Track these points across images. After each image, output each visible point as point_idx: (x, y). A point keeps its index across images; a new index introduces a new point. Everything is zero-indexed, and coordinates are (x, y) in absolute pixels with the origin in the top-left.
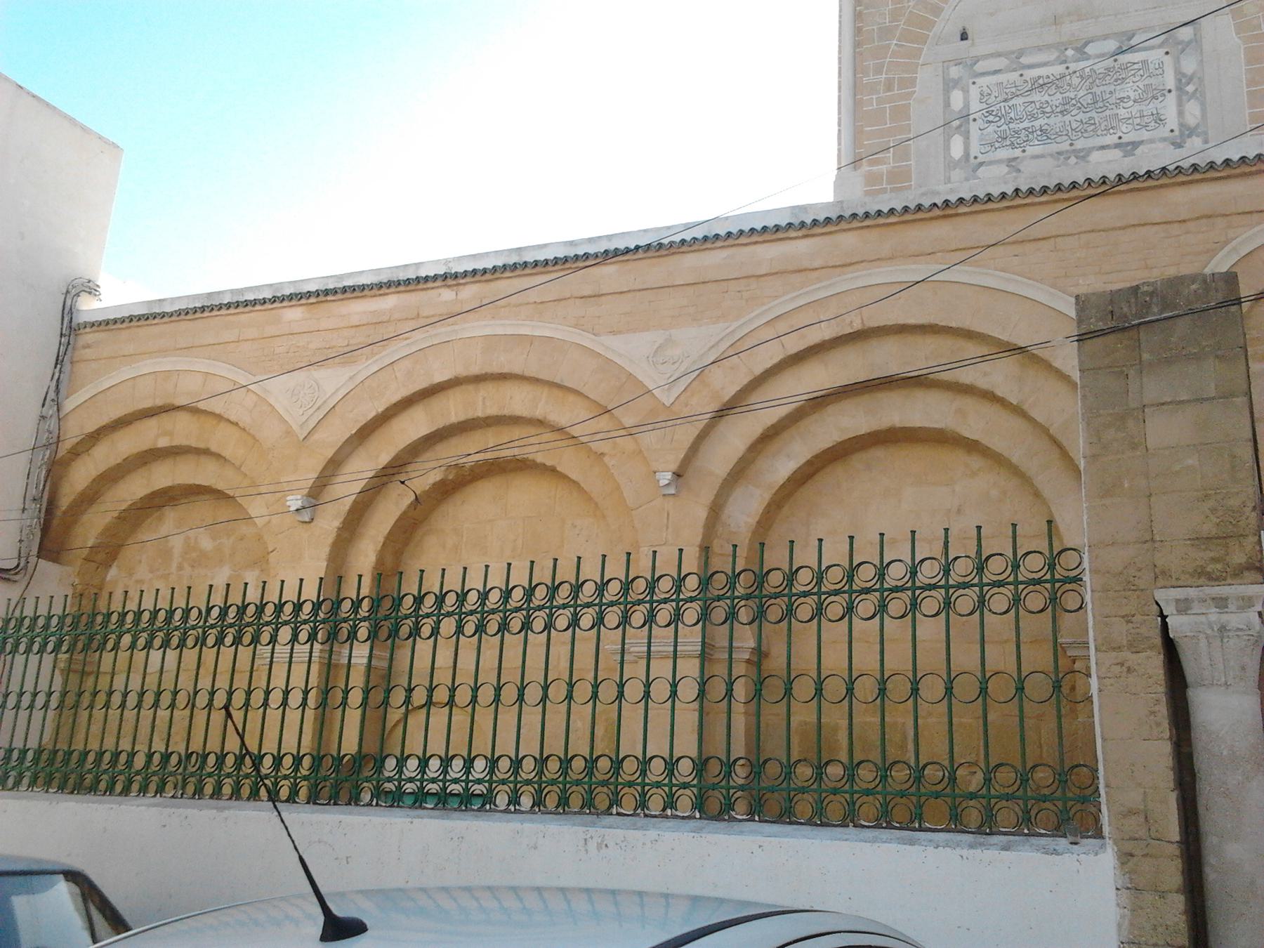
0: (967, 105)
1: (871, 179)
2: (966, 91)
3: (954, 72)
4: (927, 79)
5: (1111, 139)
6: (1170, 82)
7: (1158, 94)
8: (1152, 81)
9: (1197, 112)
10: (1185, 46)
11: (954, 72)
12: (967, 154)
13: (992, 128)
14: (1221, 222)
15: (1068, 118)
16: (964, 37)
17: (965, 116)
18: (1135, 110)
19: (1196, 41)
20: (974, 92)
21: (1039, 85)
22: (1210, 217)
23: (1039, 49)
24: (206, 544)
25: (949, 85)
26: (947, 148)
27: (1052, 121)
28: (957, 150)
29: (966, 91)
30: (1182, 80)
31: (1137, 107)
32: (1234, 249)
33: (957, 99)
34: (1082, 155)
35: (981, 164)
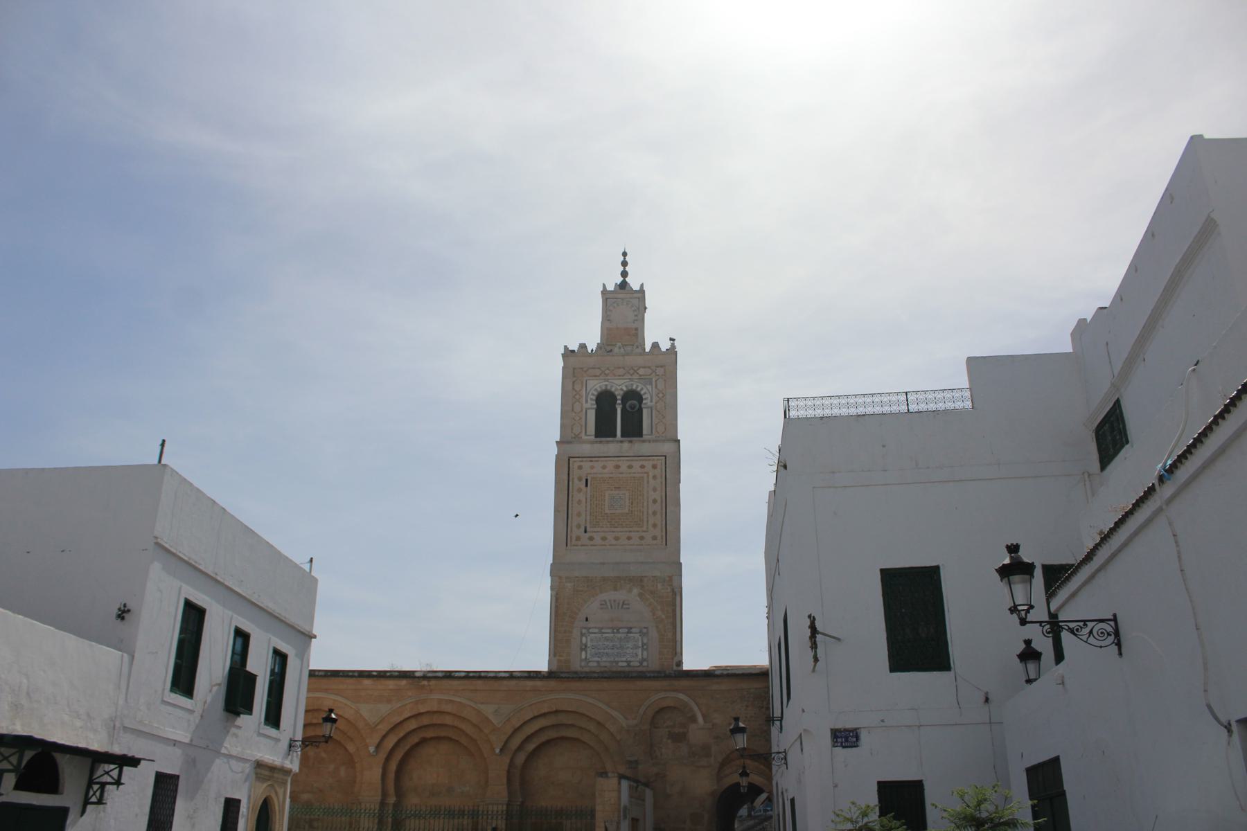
1: (559, 661)
4: (576, 632)
7: (636, 647)
21: (607, 639)
24: (324, 755)
25: (582, 635)
30: (643, 644)
34: (617, 662)
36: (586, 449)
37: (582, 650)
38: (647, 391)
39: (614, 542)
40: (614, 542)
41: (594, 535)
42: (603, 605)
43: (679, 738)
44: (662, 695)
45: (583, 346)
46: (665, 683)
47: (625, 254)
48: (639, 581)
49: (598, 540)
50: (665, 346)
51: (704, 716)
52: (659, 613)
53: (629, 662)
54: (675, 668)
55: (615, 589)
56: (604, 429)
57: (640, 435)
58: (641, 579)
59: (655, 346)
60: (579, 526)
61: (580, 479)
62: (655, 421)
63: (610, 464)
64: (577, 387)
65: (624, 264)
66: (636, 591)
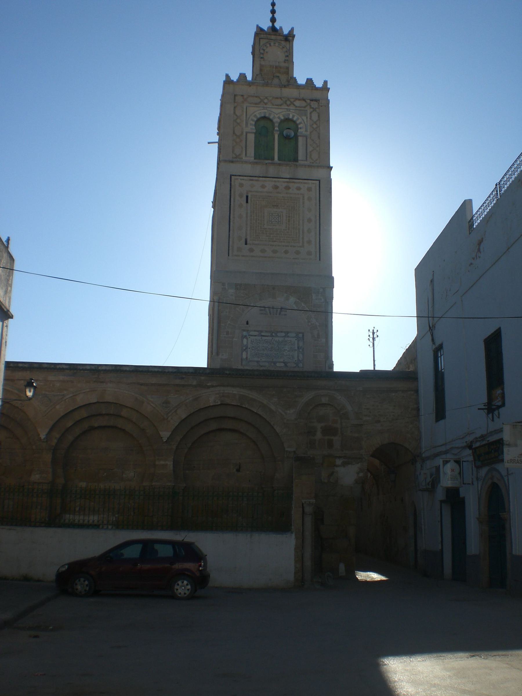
2: (247, 339)
3: (245, 333)
5: (282, 360)
6: (296, 348)
11: (245, 333)
12: (247, 358)
16: (247, 323)
23: (266, 331)
26: (242, 354)
28: (244, 356)
29: (247, 339)
33: (245, 341)
34: (275, 363)
36: (248, 169)
38: (304, 124)
45: (243, 76)
47: (273, 4)
50: (319, 84)
53: (285, 363)
54: (327, 370)
56: (263, 153)
57: (296, 160)
59: (310, 81)
61: (241, 196)
62: (310, 149)
63: (269, 184)
64: (238, 113)
65: (273, 12)
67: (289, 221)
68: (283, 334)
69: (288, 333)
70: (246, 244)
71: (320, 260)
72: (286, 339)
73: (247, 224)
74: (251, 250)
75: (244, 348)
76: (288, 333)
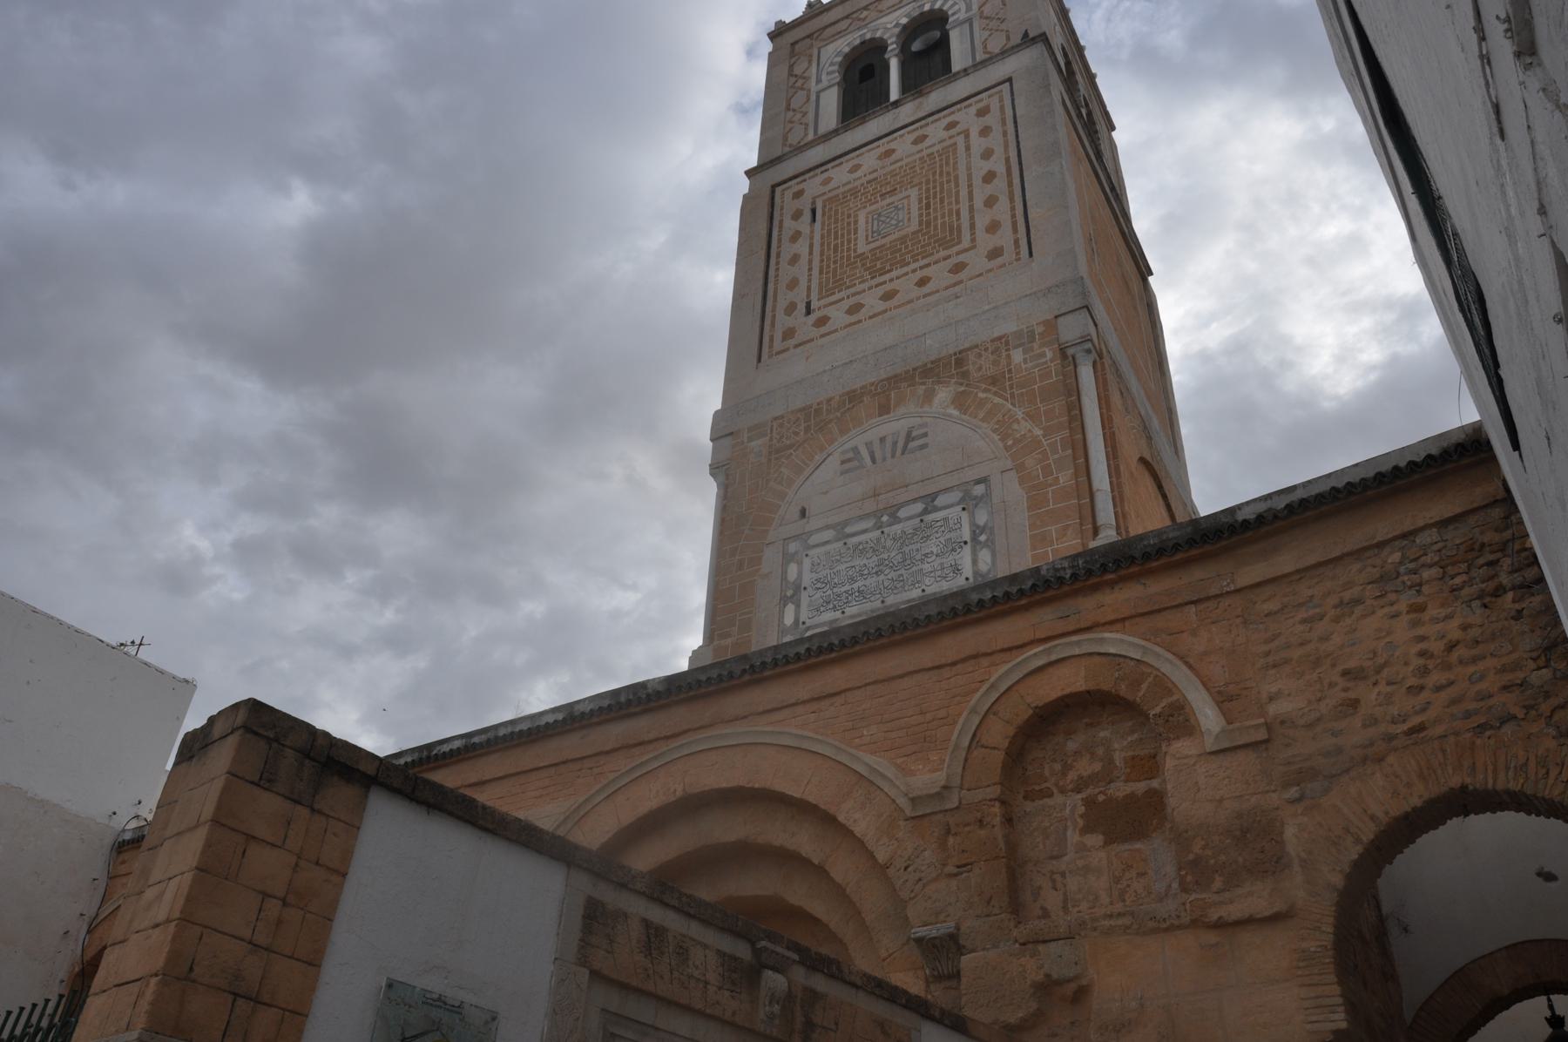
0: (800, 574)
2: (800, 564)
3: (793, 547)
4: (771, 558)
6: (966, 534)
7: (956, 546)
8: (952, 535)
9: (989, 560)
10: (978, 500)
11: (793, 547)
13: (820, 593)
14: (985, 662)
15: (882, 577)
16: (803, 513)
17: (798, 588)
18: (936, 564)
19: (988, 494)
20: (807, 563)
21: (860, 550)
22: (975, 657)
23: (861, 518)
27: (867, 582)
28: (789, 620)
30: (976, 531)
31: (939, 561)
32: (992, 686)
33: (793, 570)
35: (808, 629)
37: (785, 601)
39: (881, 306)
40: (881, 306)
41: (832, 312)
42: (851, 462)
43: (1131, 819)
44: (1035, 657)
46: (1044, 619)
48: (953, 366)
49: (838, 316)
51: (1223, 700)
52: (1024, 427)
55: (884, 409)
58: (960, 359)
60: (791, 308)
66: (943, 394)
67: (928, 206)
68: (919, 507)
69: (933, 496)
70: (808, 312)
71: (1031, 254)
72: (929, 518)
73: (810, 269)
74: (822, 321)
75: (789, 593)
76: (933, 496)
